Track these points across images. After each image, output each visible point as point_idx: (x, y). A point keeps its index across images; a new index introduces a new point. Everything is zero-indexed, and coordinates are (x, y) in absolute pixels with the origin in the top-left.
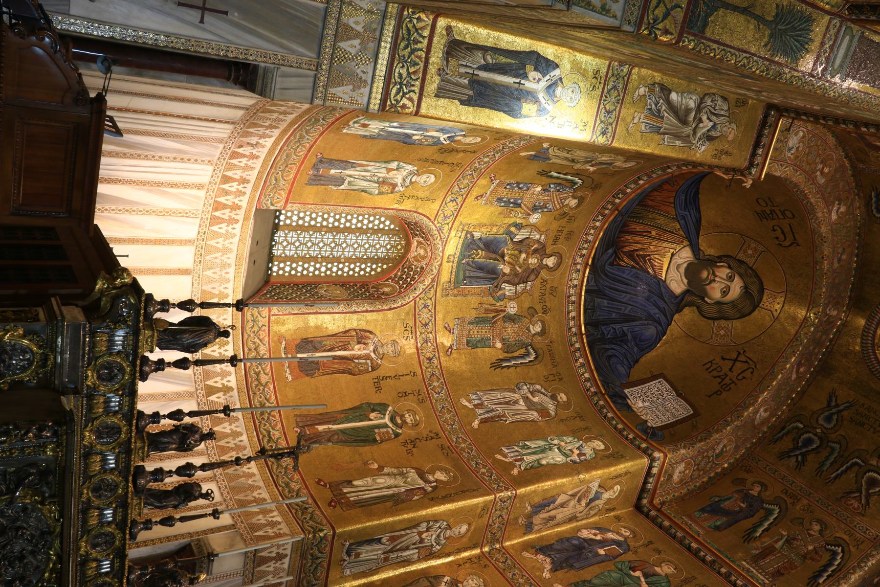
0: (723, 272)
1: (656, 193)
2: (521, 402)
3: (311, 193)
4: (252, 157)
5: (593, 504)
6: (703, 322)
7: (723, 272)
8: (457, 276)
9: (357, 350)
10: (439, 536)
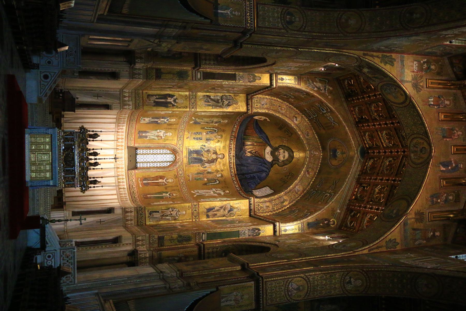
0: (282, 151)
1: (247, 131)
2: (212, 192)
3: (140, 140)
4: (122, 132)
5: (230, 213)
6: (279, 168)
7: (282, 151)
8: (189, 162)
9: (160, 181)
10: (176, 213)
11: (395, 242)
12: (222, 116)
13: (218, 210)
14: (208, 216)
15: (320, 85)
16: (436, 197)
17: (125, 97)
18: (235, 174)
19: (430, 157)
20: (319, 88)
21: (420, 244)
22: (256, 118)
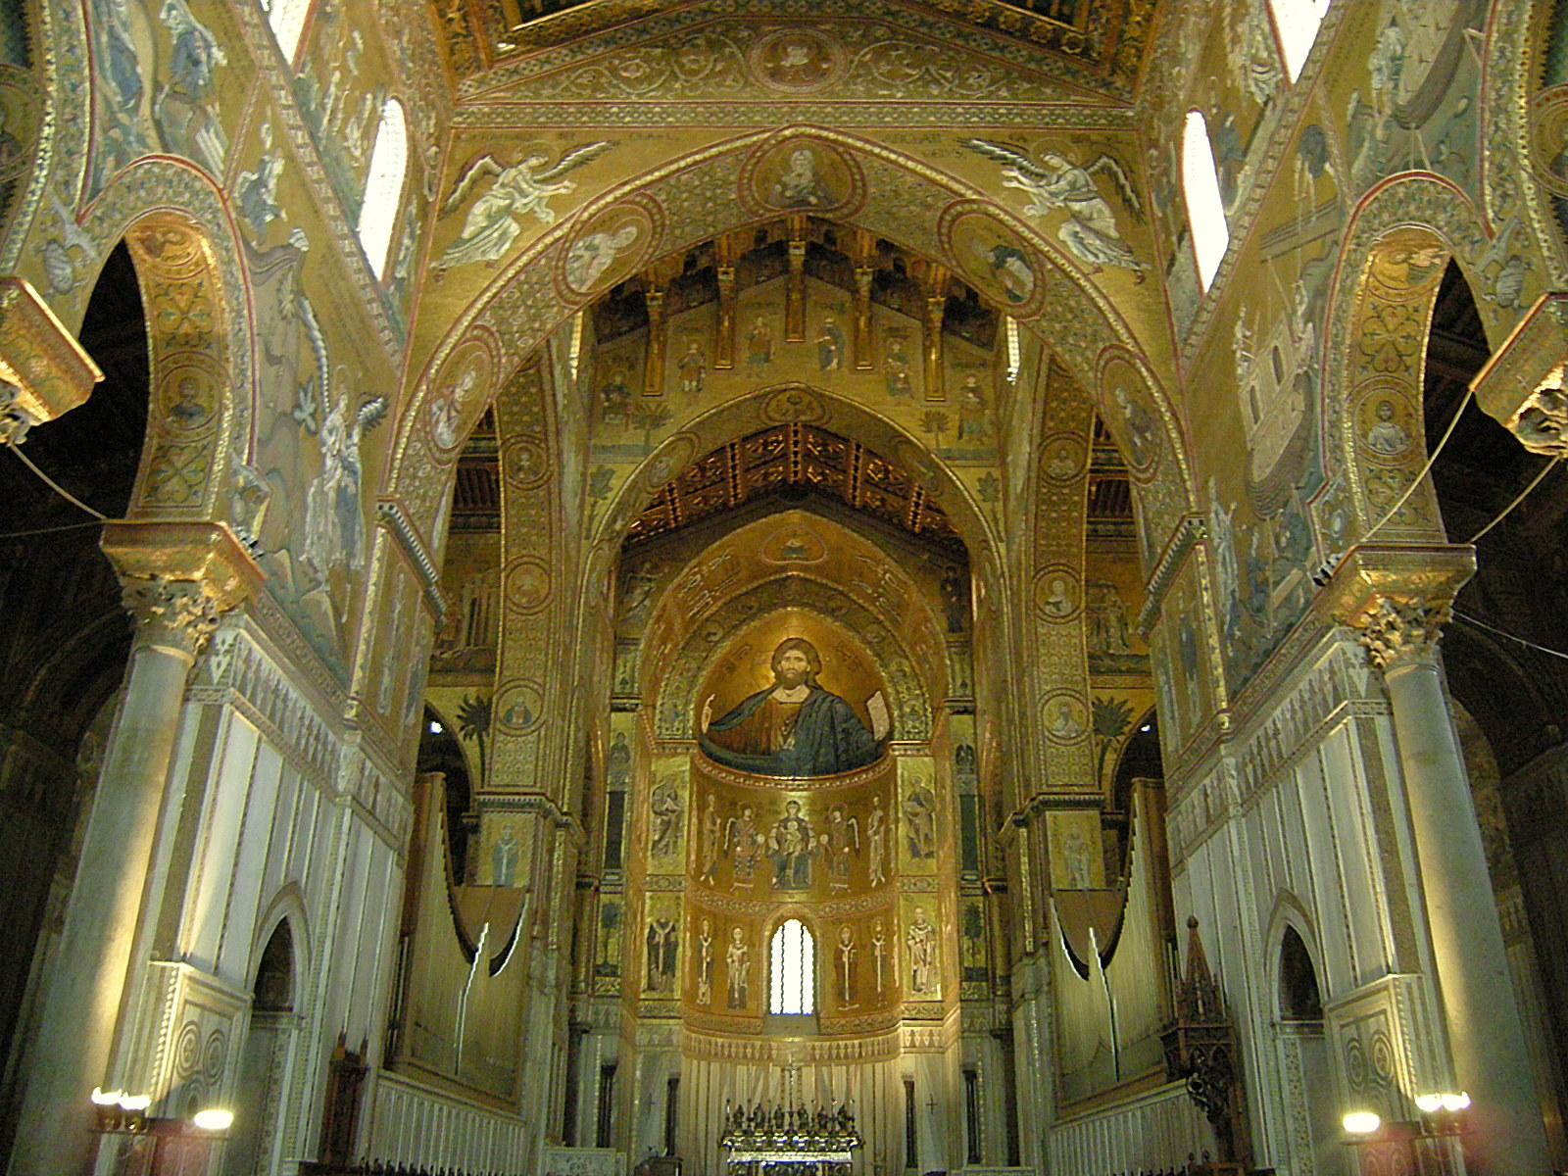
3: (751, 1005)
4: (730, 1046)
9: (845, 959)
11: (986, 481)
12: (699, 809)
13: (917, 831)
14: (929, 855)
15: (638, 591)
16: (895, 382)
17: (651, 1039)
18: (837, 778)
19: (808, 391)
20: (647, 594)
21: (992, 423)
22: (705, 727)
